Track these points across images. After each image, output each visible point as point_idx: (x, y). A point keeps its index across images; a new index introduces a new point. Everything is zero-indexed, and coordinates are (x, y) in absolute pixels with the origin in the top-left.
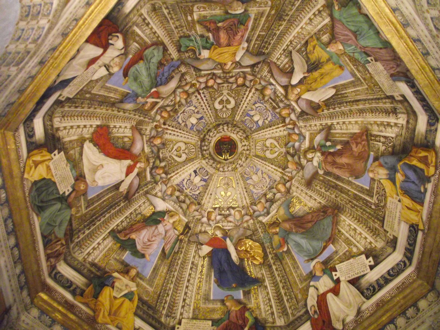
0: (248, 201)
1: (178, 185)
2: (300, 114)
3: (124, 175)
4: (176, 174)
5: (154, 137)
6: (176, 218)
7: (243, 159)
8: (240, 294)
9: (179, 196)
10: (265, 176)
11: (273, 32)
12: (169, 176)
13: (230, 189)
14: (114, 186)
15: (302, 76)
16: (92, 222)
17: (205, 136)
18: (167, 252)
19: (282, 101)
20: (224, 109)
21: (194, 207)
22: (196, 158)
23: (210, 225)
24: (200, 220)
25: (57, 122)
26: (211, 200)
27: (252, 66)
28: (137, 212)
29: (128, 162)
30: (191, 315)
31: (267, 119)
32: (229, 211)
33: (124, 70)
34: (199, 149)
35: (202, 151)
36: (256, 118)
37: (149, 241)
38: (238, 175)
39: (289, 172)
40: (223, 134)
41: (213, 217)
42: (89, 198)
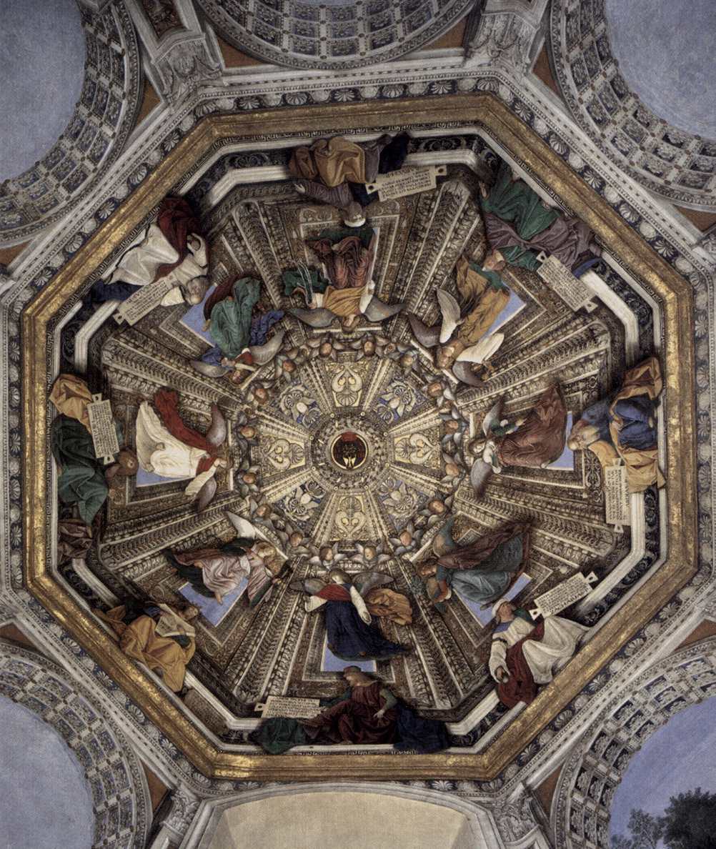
0: (385, 532)
1: (275, 504)
2: (457, 388)
5: (243, 426)
6: (270, 552)
7: (377, 469)
11: (408, 263)
12: (262, 490)
13: (356, 515)
14: (177, 483)
15: (454, 326)
16: (138, 526)
21: (299, 540)
23: (324, 568)
24: (308, 559)
25: (106, 357)
27: (384, 323)
29: (201, 453)
30: (284, 692)
32: (355, 547)
35: (314, 456)
36: (393, 405)
39: (448, 482)
41: (329, 557)
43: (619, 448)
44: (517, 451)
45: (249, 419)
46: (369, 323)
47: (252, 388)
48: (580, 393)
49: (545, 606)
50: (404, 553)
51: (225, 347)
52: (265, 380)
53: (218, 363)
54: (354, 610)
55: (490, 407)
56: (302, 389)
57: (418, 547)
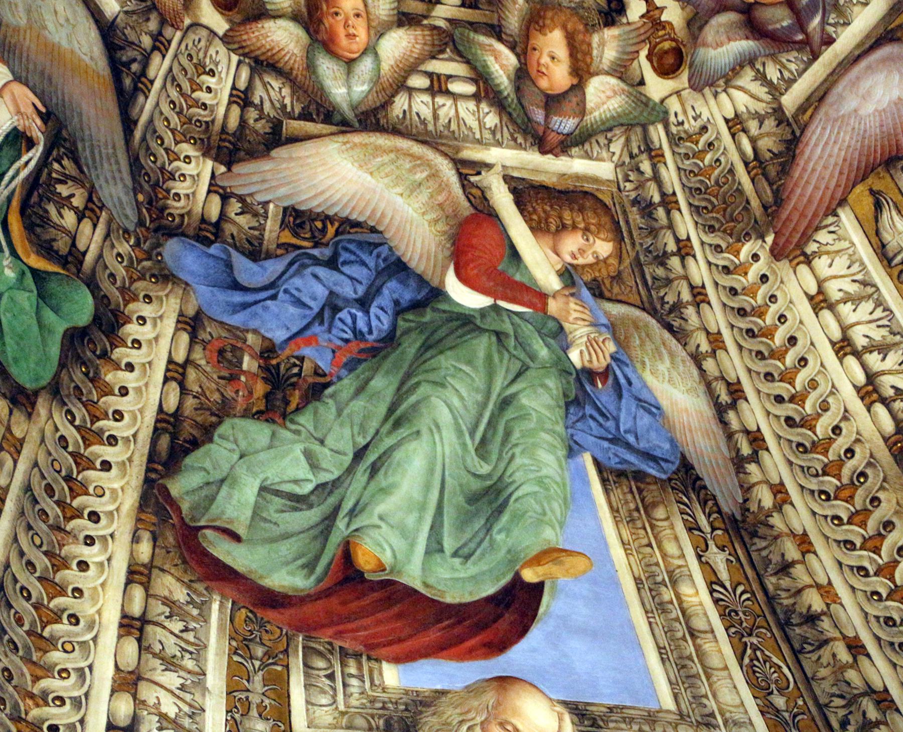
33: (499, 646)
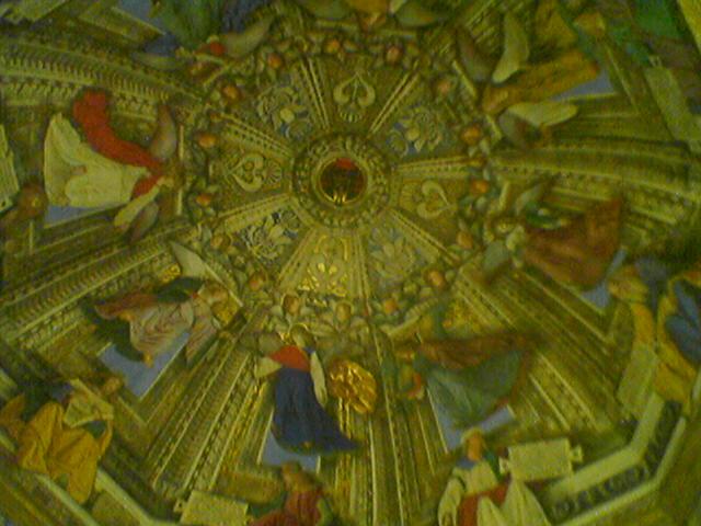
0: (367, 292)
1: (236, 235)
3: (128, 198)
4: (236, 213)
5: (202, 133)
7: (373, 210)
8: (316, 465)
9: (235, 257)
10: (408, 249)
12: (221, 215)
13: (336, 261)
15: (515, 68)
16: (46, 274)
17: (305, 151)
18: (189, 359)
19: (467, 111)
20: (352, 105)
21: (261, 282)
22: (282, 190)
26: (296, 276)
27: (422, 30)
28: (144, 271)
29: (139, 172)
31: (432, 141)
34: (290, 175)
35: (295, 178)
36: (411, 136)
37: (158, 329)
38: (357, 238)
40: (340, 154)
41: (294, 308)
42: (47, 226)
43: (661, 331)
44: (546, 253)
45: (211, 124)
46: (398, 26)
47: (219, 85)
48: (643, 233)
49: (522, 462)
50: (384, 322)
51: (182, 34)
52: (240, 75)
53: (170, 54)
54: (310, 383)
55: (534, 184)
56: (291, 92)
57: (401, 320)
